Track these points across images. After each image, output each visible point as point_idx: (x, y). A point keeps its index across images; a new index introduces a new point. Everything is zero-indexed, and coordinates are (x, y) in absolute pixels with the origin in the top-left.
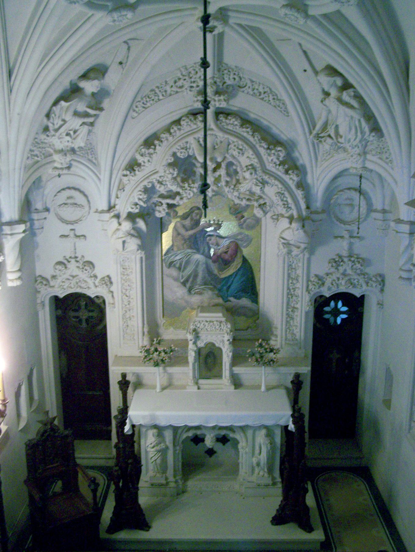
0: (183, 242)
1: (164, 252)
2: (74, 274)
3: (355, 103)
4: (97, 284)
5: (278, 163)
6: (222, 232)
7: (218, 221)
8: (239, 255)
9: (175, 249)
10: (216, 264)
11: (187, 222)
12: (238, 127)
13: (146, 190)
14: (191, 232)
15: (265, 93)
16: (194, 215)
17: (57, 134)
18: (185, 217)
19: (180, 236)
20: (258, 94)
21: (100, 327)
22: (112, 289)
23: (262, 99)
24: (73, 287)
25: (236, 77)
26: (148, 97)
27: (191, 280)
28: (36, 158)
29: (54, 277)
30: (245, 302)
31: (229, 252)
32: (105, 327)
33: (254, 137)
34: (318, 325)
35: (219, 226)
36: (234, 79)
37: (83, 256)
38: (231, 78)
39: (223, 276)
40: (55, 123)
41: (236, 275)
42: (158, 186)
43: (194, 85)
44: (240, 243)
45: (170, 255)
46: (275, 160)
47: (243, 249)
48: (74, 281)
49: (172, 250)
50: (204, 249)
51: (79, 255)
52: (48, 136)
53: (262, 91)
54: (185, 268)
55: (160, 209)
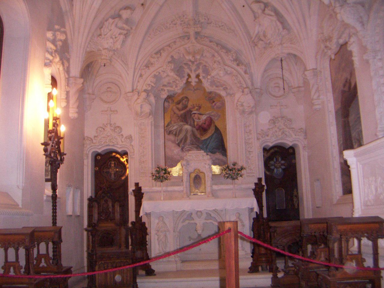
0: (177, 118)
1: (166, 126)
2: (109, 134)
3: (273, 14)
4: (123, 141)
5: (232, 60)
6: (201, 111)
7: (199, 104)
8: (212, 125)
9: (172, 122)
10: (199, 131)
11: (180, 106)
12: (208, 42)
13: (155, 76)
14: (182, 112)
15: (222, 26)
16: (184, 101)
17: (106, 36)
18: (178, 103)
19: (175, 115)
20: (219, 27)
21: (123, 178)
22: (132, 144)
23: (222, 29)
24: (107, 142)
25: (206, 18)
26: (157, 30)
27: (183, 141)
28: (93, 49)
29: (95, 137)
30: (218, 156)
31: (206, 124)
32: (127, 178)
33: (218, 47)
34: (268, 173)
35: (200, 107)
36: (205, 19)
37: (115, 123)
38: (203, 18)
39: (203, 138)
40: (105, 31)
41: (212, 138)
42: (162, 73)
43: (183, 22)
44: (213, 117)
45: (169, 127)
46: (231, 58)
47: (215, 121)
48: (109, 138)
49: (171, 123)
50: (191, 122)
51: (112, 123)
52: (100, 38)
53: (220, 25)
54: (179, 134)
55: (163, 92)
